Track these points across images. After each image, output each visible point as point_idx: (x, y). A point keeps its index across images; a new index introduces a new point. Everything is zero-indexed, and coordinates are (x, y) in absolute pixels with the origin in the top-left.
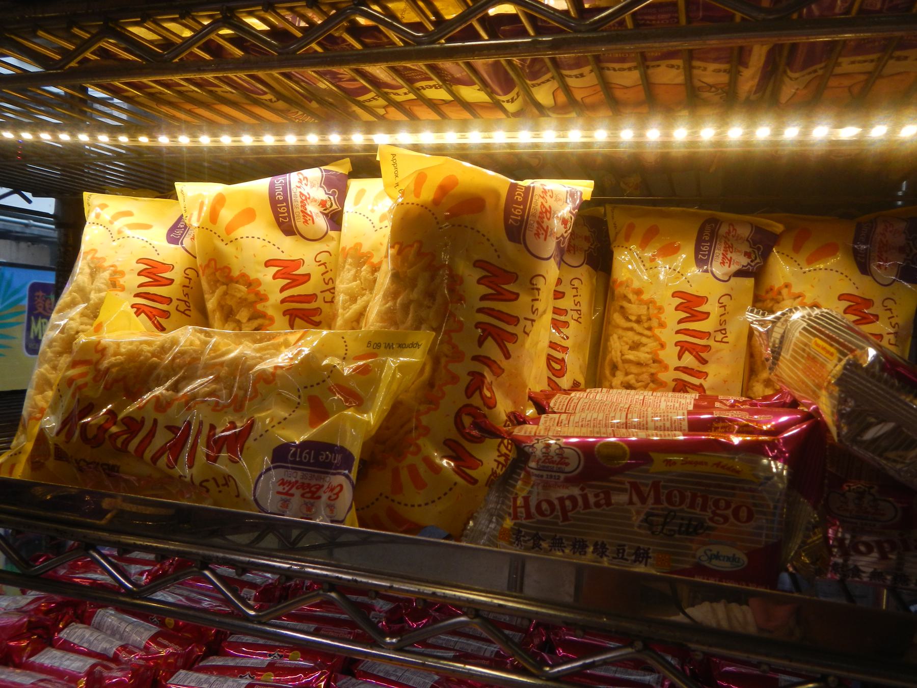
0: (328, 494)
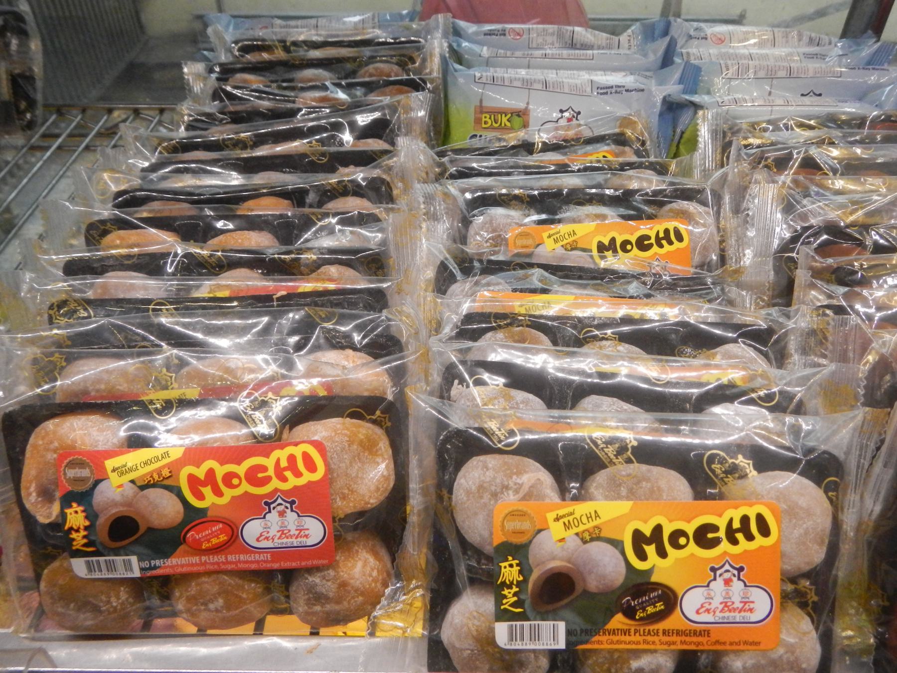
0: (713, 607)
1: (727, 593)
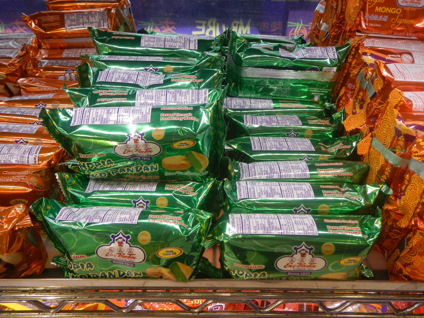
1: (120, 250)
